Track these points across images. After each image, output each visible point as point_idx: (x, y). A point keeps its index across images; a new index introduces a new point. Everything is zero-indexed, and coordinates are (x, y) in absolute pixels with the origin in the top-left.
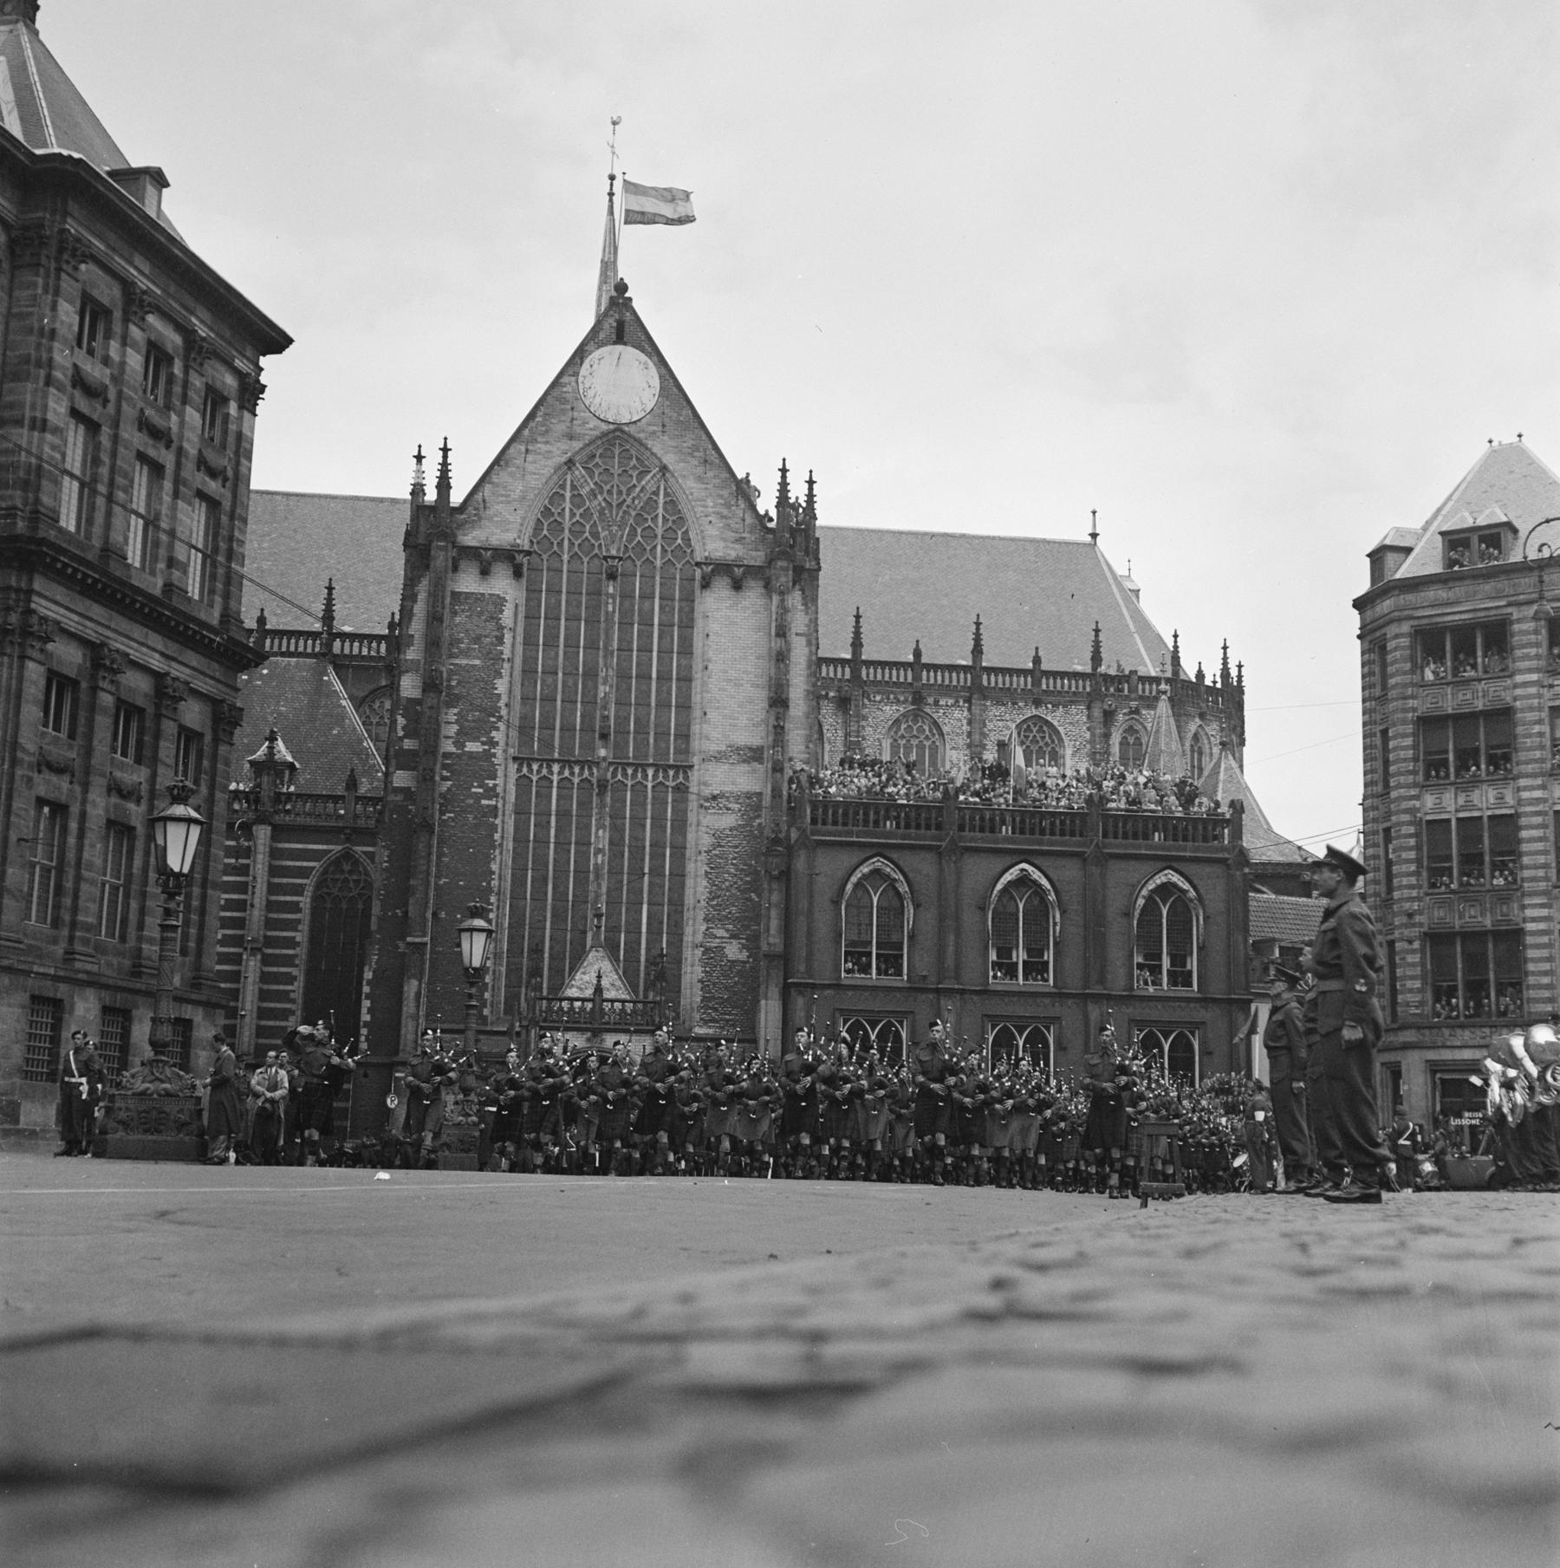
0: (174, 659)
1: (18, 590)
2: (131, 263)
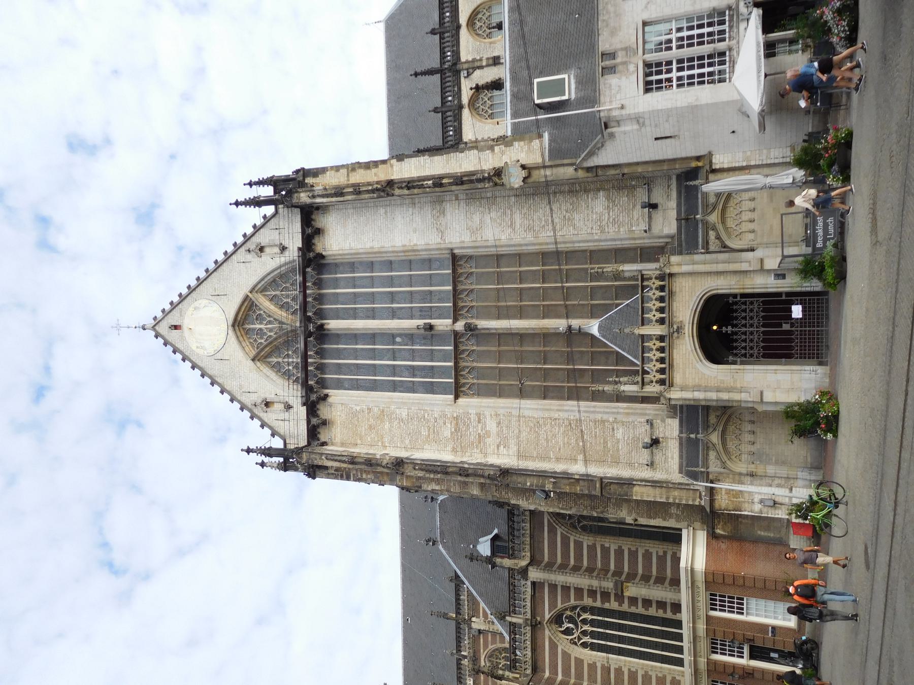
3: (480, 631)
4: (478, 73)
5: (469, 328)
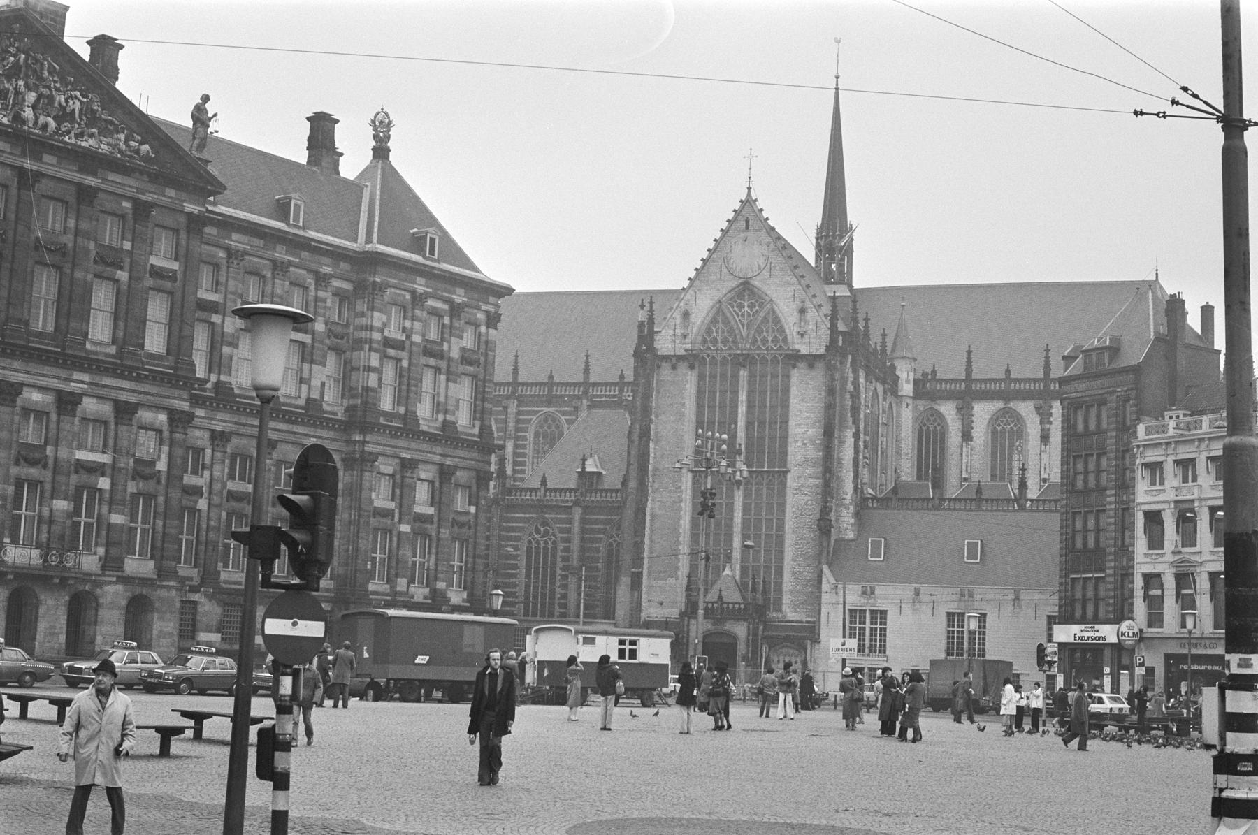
0: (447, 456)
1: (359, 441)
2: (415, 283)
3: (506, 408)
4: (1037, 419)
5: (739, 483)
